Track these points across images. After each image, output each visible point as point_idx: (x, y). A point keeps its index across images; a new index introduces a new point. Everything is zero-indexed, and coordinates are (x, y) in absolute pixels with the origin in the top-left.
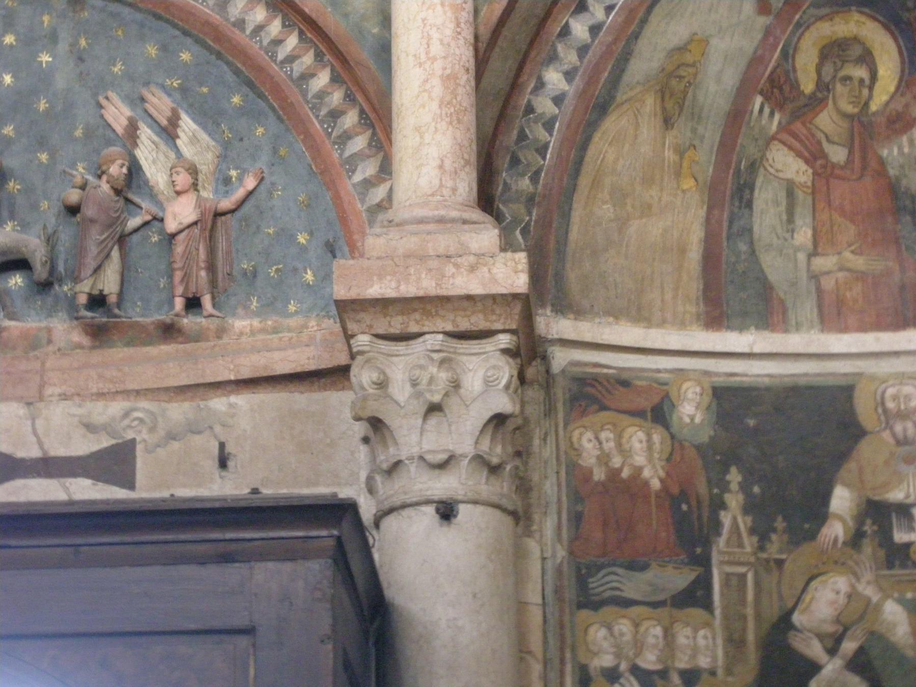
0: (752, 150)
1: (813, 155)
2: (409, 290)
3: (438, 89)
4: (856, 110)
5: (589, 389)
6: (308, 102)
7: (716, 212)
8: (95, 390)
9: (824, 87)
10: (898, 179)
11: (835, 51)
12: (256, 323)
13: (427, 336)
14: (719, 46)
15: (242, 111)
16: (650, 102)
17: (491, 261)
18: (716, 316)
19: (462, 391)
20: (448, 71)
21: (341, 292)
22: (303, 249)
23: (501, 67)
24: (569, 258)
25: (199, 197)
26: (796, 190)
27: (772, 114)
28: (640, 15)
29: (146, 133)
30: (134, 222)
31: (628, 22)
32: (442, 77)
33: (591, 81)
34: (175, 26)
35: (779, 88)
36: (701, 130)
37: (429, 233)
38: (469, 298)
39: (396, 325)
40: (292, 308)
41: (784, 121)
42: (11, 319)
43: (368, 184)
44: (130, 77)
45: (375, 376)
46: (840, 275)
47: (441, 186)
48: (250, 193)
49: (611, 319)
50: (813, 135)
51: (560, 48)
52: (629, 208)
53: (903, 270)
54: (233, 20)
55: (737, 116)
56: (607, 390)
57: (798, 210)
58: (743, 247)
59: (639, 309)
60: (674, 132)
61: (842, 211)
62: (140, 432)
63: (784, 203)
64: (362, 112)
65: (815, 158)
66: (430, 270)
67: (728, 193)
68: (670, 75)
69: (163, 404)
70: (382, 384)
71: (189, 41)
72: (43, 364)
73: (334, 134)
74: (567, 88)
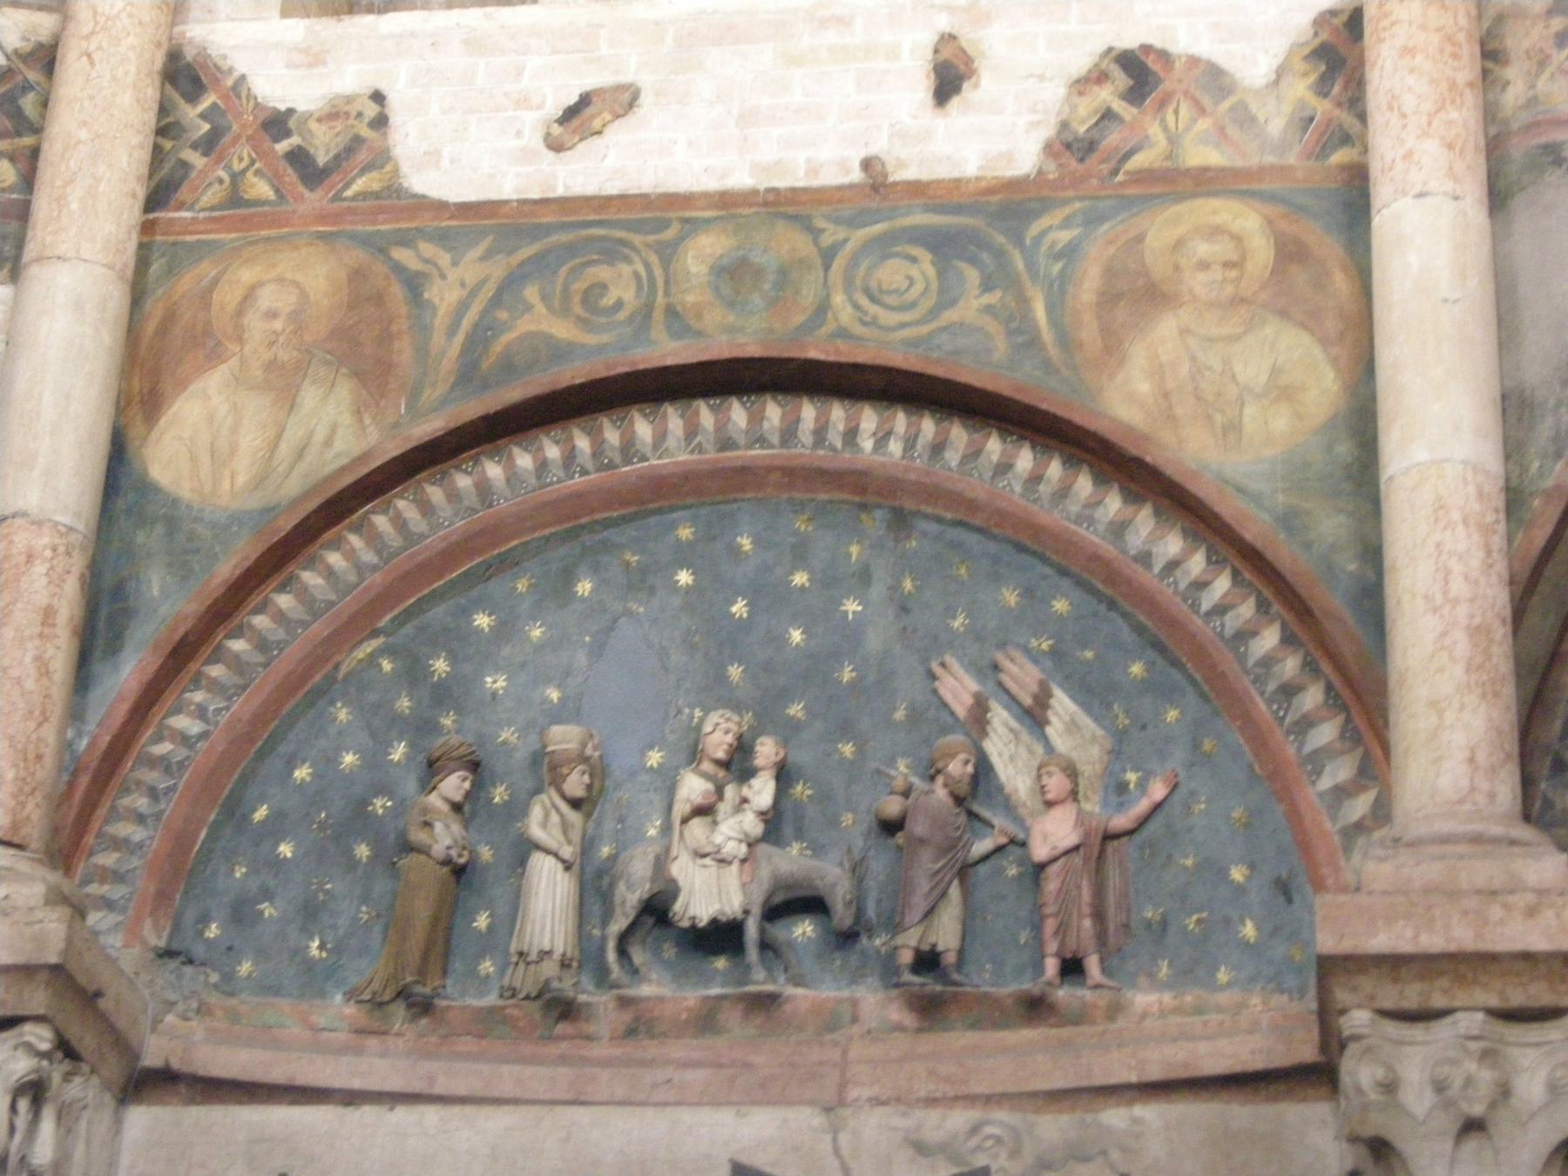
2: (1432, 942)
3: (1461, 644)
6: (1247, 672)
8: (922, 1094)
12: (1167, 998)
13: (1459, 1015)
15: (1147, 686)
17: (1560, 901)
19: (1513, 1101)
20: (1477, 621)
21: (1327, 942)
22: (1240, 890)
25: (1080, 812)
29: (1000, 716)
30: (981, 846)
32: (1468, 627)
34: (1045, 560)
37: (1461, 857)
38: (1528, 957)
39: (1411, 995)
40: (1223, 976)
42: (797, 985)
43: (1341, 793)
44: (976, 634)
45: (1380, 1073)
47: (1473, 789)
48: (1158, 807)
54: (1133, 552)
62: (996, 1156)
64: (1329, 688)
66: (1465, 913)
69: (1031, 1117)
70: (1390, 1087)
71: (1065, 583)
72: (845, 1052)
73: (1288, 720)
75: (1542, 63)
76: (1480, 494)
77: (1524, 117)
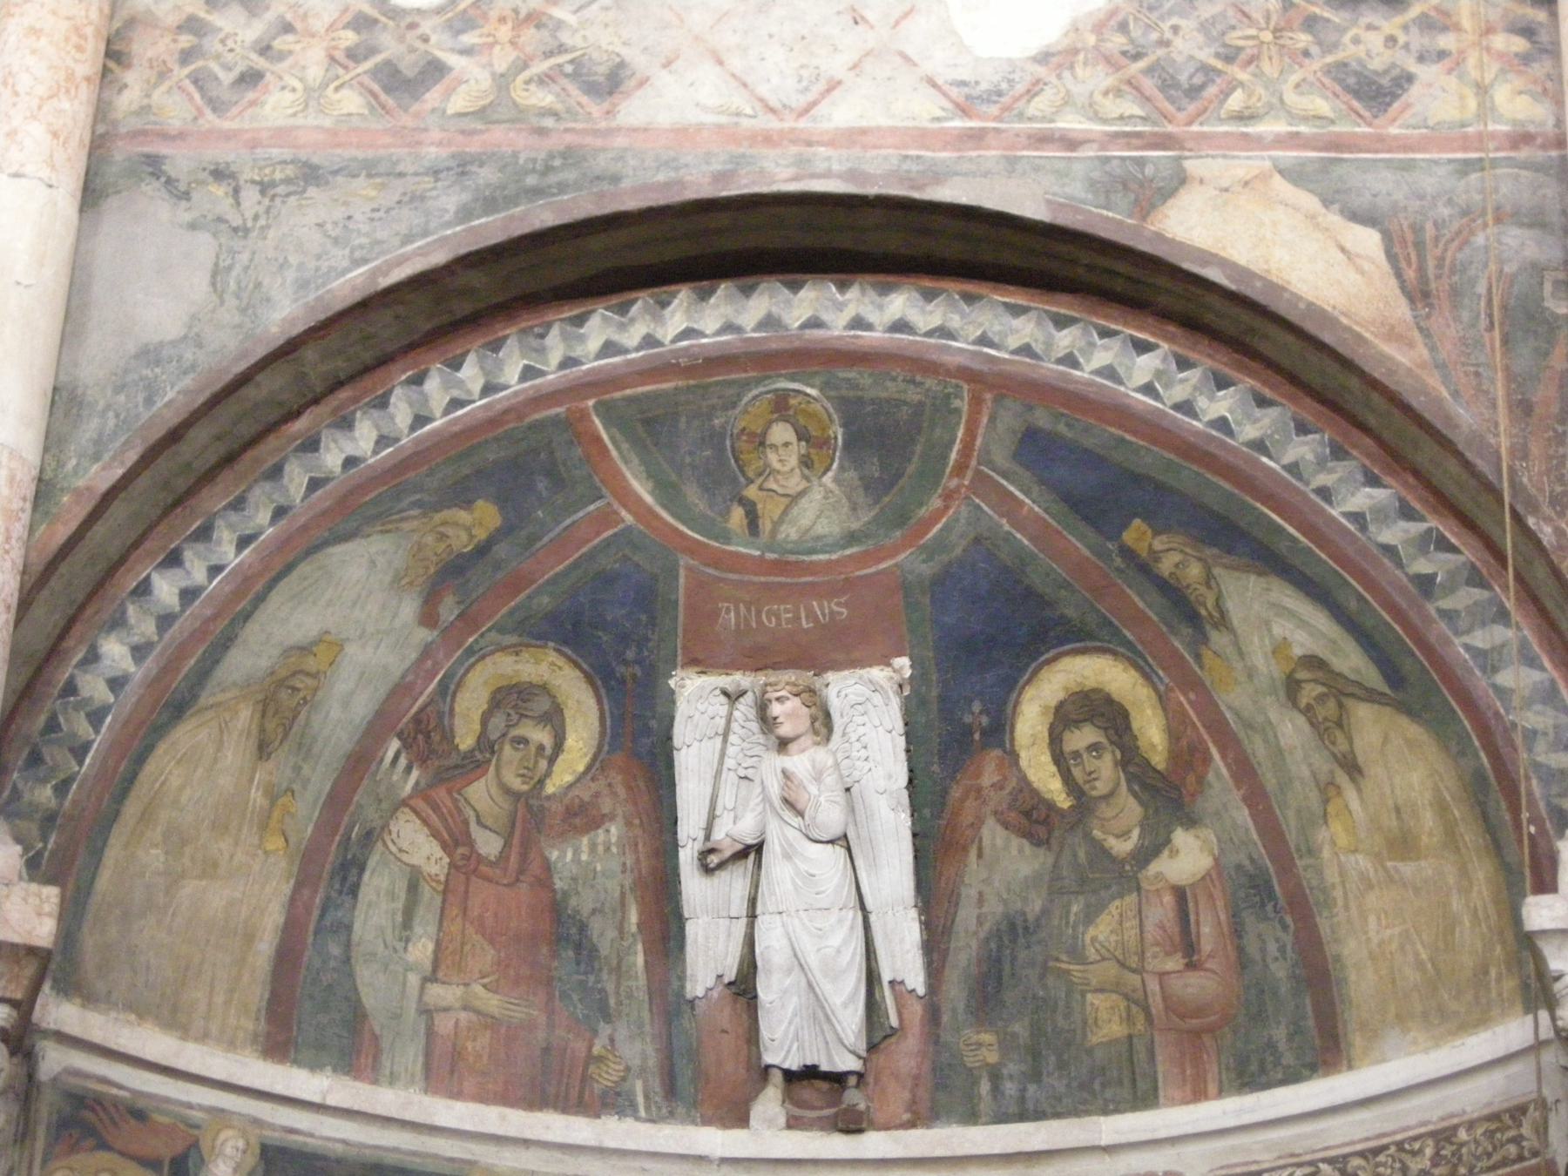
0: (372, 815)
1: (455, 839)
4: (525, 787)
5: (88, 1115)
7: (306, 892)
9: (487, 746)
10: (565, 893)
11: (514, 699)
14: (357, 655)
16: (245, 715)
18: (279, 1043)
23: (46, 616)
24: (89, 917)
26: (422, 883)
27: (408, 769)
28: (259, 587)
31: (238, 594)
33: (168, 669)
35: (425, 734)
36: (306, 770)
41: (423, 783)
46: (463, 1015)
49: (133, 1017)
50: (460, 811)
51: (131, 610)
52: (186, 861)
53: (551, 1026)
55: (359, 762)
56: (112, 1118)
57: (421, 911)
58: (335, 950)
59: (175, 1009)
60: (270, 765)
61: (481, 929)
63: (403, 895)
65: (457, 844)
67: (328, 867)
68: (281, 683)
74: (132, 669)
75: (163, 75)
76: (12, 480)
77: (136, 123)
